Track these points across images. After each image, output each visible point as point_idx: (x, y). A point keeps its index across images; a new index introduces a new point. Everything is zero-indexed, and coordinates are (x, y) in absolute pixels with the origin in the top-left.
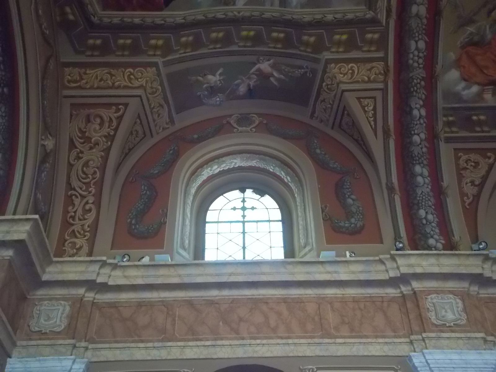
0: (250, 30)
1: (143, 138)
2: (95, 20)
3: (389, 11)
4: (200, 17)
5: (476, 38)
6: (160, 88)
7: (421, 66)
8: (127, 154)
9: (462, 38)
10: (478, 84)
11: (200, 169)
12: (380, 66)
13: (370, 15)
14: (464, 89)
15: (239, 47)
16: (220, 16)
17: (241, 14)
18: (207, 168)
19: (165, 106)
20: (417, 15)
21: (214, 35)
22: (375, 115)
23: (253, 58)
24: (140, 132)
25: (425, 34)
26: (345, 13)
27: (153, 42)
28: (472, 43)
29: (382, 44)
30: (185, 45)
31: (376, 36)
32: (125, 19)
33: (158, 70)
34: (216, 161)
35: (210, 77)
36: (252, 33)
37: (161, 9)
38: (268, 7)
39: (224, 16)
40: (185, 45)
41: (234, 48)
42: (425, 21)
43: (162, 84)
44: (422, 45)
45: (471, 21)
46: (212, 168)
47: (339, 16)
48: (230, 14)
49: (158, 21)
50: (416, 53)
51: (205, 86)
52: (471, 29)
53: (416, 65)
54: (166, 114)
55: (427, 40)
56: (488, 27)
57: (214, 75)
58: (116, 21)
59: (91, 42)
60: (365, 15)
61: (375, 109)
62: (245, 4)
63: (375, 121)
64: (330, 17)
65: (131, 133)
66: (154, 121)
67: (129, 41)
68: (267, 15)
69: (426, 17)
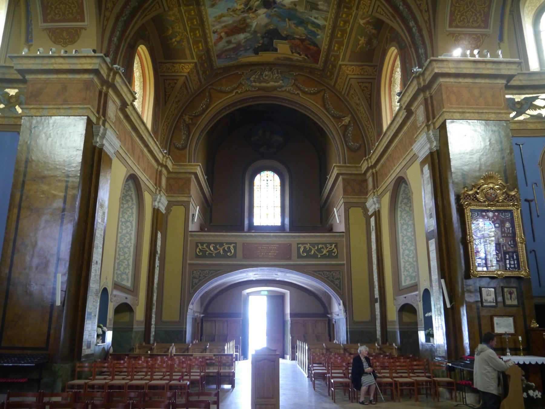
1: (371, 84)
4: (328, 39)
6: (352, 67)
8: (370, 98)
11: (392, 79)
15: (348, 27)
16: (330, 31)
18: (395, 74)
19: (364, 67)
21: (339, 36)
22: (385, 13)
24: (367, 85)
30: (339, 48)
33: (343, 65)
34: (394, 68)
35: (360, 42)
40: (339, 48)
41: (348, 30)
43: (351, 65)
46: (397, 71)
48: (330, 28)
51: (364, 45)
57: (360, 40)
61: (383, 11)
63: (388, 16)
65: (363, 90)
66: (368, 75)
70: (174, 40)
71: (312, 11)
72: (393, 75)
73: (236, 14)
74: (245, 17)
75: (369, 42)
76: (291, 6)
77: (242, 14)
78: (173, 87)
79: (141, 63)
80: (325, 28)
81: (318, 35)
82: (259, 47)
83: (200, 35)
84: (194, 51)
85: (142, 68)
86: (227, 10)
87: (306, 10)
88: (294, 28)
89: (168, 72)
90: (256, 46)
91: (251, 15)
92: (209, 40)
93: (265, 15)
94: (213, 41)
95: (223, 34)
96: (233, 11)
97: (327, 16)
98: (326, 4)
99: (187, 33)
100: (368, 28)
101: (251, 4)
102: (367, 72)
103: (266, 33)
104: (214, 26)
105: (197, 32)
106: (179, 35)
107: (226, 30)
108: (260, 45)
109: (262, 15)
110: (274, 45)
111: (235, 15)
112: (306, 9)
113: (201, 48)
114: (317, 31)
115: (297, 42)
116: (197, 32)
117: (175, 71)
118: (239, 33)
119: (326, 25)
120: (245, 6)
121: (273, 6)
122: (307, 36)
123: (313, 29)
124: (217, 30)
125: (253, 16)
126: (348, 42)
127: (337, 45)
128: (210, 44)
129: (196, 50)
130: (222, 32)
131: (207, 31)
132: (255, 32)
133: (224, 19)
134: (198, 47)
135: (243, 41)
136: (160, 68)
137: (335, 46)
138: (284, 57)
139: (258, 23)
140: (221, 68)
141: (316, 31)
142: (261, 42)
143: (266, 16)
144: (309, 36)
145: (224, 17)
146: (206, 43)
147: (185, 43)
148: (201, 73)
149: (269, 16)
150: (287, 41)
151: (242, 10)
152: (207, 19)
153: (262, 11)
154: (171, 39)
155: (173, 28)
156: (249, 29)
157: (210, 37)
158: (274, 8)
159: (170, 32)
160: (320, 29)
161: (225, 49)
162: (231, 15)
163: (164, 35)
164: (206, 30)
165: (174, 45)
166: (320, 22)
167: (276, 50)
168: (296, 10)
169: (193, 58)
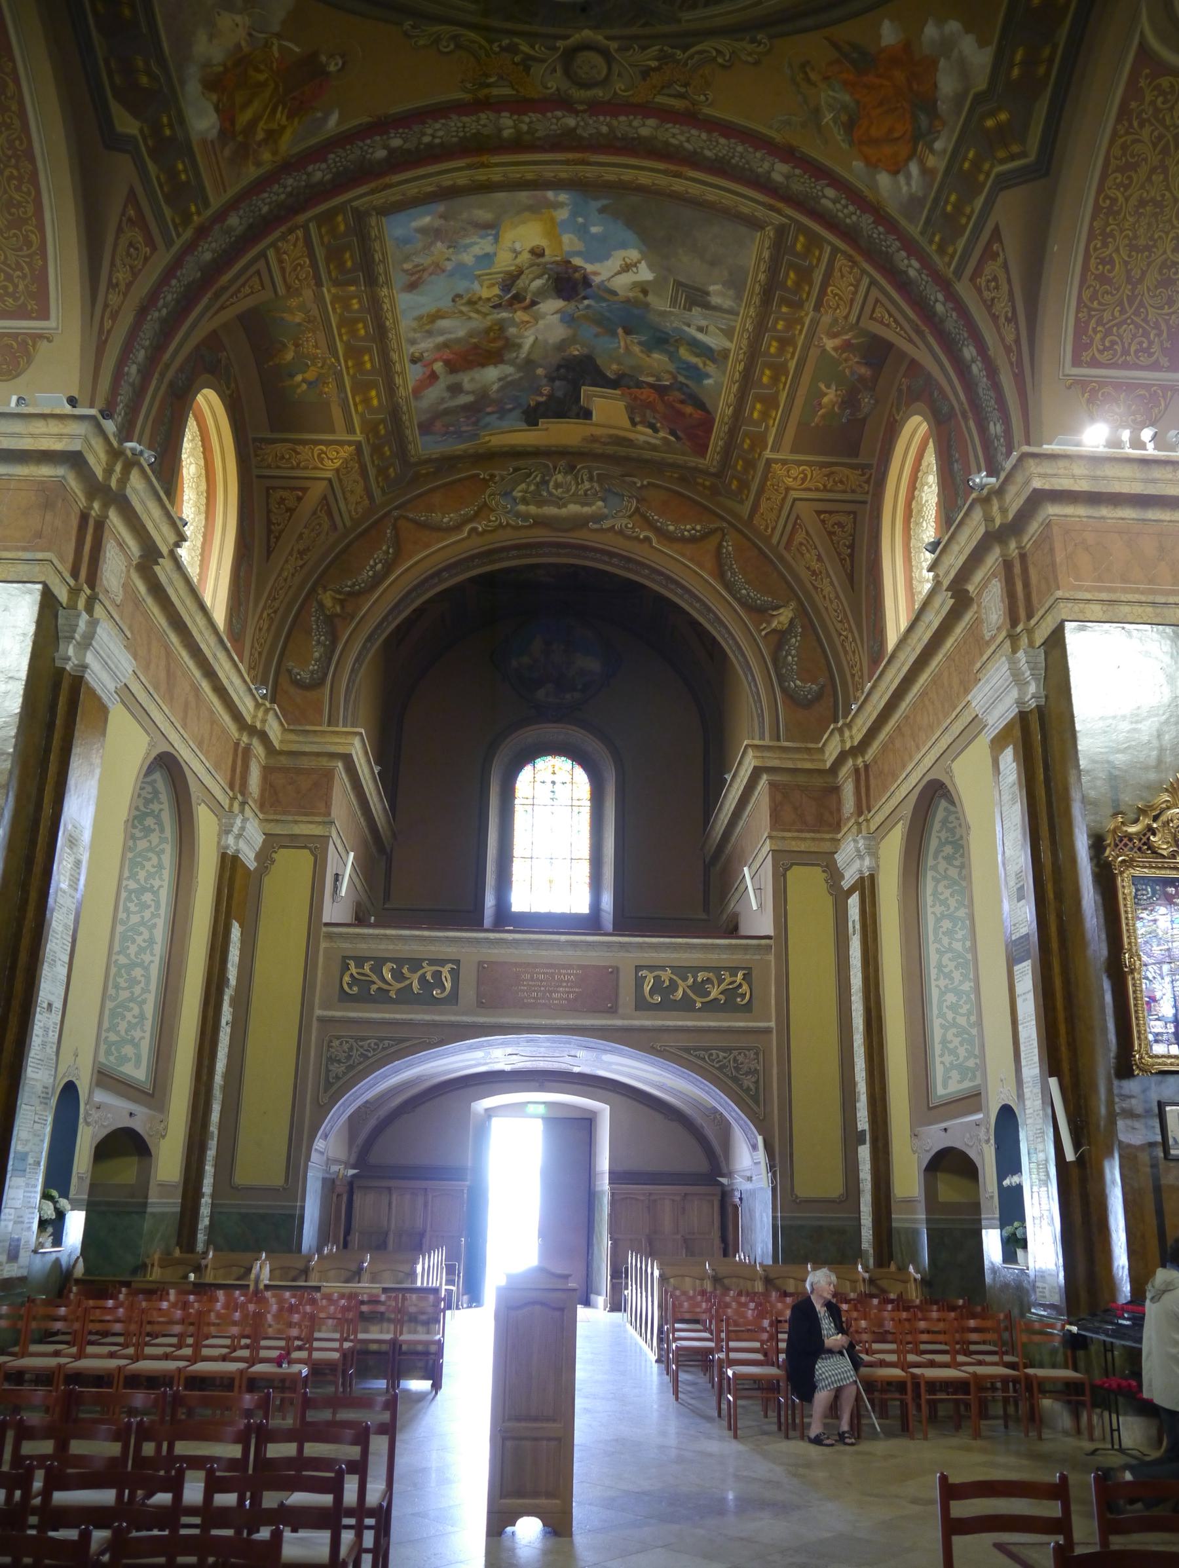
1: (855, 518)
3: (771, 208)
4: (735, 388)
5: (844, 118)
7: (858, 212)
8: (851, 556)
9: (839, 136)
10: (909, 158)
11: (914, 504)
12: (840, 261)
13: (770, 231)
14: (908, 184)
15: (792, 358)
16: (741, 367)
19: (834, 469)
20: (787, 177)
21: (765, 380)
22: (896, 321)
23: (814, 353)
24: (842, 518)
26: (760, 259)
28: (850, 126)
29: (814, 241)
30: (765, 415)
33: (776, 461)
34: (920, 474)
35: (825, 400)
37: (713, 420)
40: (765, 415)
41: (792, 365)
42: (798, 171)
43: (799, 463)
44: (830, 192)
45: (817, 112)
47: (763, 267)
48: (741, 357)
50: (839, 206)
52: (828, 117)
53: (854, 218)
54: (846, 471)
56: (831, 93)
57: (825, 394)
61: (890, 315)
63: (902, 329)
64: (762, 277)
65: (831, 534)
66: (845, 492)
69: (794, 168)
70: (299, 378)
71: (690, 310)
72: (916, 493)
73: (478, 312)
74: (503, 320)
75: (850, 401)
76: (631, 294)
78: (290, 511)
79: (203, 440)
80: (726, 357)
81: (708, 376)
82: (539, 404)
83: (373, 366)
84: (356, 410)
85: (204, 453)
86: (453, 301)
88: (640, 355)
89: (278, 467)
90: (532, 403)
91: (520, 316)
92: (398, 380)
93: (558, 316)
95: (438, 367)
96: (471, 303)
97: (733, 324)
98: (731, 292)
99: (338, 360)
100: (846, 360)
102: (841, 482)
103: (559, 367)
104: (413, 342)
105: (366, 358)
106: (314, 364)
107: (447, 354)
108: (543, 399)
110: (583, 401)
112: (674, 303)
113: (375, 402)
114: (705, 364)
115: (646, 394)
116: (366, 358)
117: (298, 464)
118: (483, 365)
119: (729, 350)
120: (502, 290)
122: (675, 378)
123: (694, 360)
124: (422, 354)
125: (526, 318)
126: (791, 398)
127: (758, 406)
128: (402, 392)
129: (360, 408)
130: (436, 360)
131: (395, 356)
132: (529, 364)
133: (443, 323)
134: (367, 401)
135: (495, 387)
136: (256, 455)
137: (753, 408)
138: (611, 436)
139: (540, 337)
140: (429, 461)
141: (701, 365)
142: (546, 390)
143: (562, 320)
144: (681, 379)
145: (443, 317)
146: (391, 388)
147: (330, 389)
148: (372, 472)
149: (569, 320)
150: (618, 392)
151: (497, 301)
152: (396, 322)
153: (551, 306)
154: (292, 376)
155: (297, 345)
156: (514, 355)
157: (403, 373)
158: (585, 298)
159: (289, 355)
160: (714, 361)
162: (461, 312)
163: (271, 364)
164: (392, 353)
165: (299, 391)
166: (714, 341)
167: (587, 414)
168: (647, 306)
169: (351, 430)
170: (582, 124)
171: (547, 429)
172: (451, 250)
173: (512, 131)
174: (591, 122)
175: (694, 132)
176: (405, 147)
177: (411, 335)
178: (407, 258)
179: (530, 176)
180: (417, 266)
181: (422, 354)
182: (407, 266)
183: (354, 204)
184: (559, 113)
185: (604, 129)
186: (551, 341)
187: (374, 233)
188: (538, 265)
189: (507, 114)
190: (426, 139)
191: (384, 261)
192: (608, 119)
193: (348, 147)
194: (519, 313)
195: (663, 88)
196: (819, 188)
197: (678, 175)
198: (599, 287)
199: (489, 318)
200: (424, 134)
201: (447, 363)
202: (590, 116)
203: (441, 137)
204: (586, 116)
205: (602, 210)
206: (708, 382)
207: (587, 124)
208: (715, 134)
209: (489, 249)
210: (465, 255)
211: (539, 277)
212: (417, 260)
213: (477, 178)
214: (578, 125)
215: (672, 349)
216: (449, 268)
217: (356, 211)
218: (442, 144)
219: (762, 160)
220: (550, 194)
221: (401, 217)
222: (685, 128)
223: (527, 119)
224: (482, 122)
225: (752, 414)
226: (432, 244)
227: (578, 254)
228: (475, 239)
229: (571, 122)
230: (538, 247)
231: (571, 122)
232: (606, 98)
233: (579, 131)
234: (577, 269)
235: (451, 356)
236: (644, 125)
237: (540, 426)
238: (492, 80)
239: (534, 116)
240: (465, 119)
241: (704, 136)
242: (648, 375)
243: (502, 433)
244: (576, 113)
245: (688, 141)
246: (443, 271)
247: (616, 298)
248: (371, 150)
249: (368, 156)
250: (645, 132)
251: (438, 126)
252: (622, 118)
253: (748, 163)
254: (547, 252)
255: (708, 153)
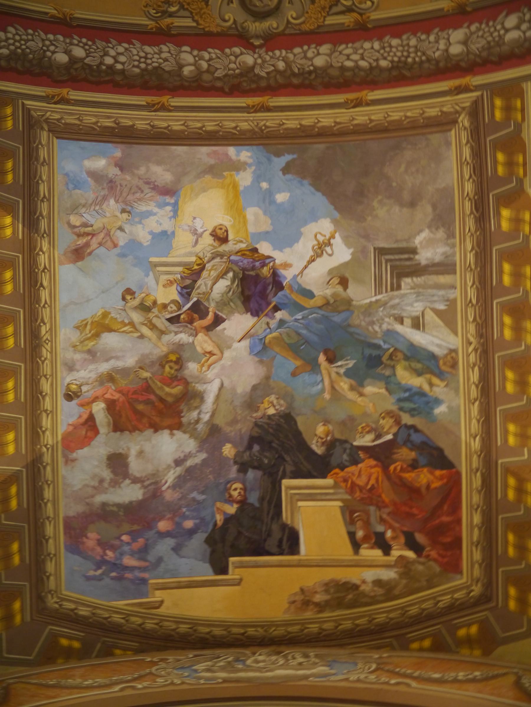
0: (502, 324)
2: (477, 590)
13: (464, 120)
16: (475, 376)
17: (472, 339)
21: (510, 388)
25: (494, 20)
26: (461, 163)
27: (511, 495)
31: (498, 102)
32: (475, 539)
36: (507, 320)
38: (456, 294)
39: (476, 369)
48: (472, 358)
49: (477, 482)
55: (504, 14)
58: (477, 556)
59: (512, 605)
60: (465, 128)
62: (456, 333)
64: (469, 187)
67: (511, 537)
68: (472, 294)
69: (468, 27)
71: (399, 287)
73: (153, 327)
74: (180, 347)
76: (329, 292)
77: (173, 328)
80: (454, 365)
81: (438, 402)
82: (228, 519)
86: (124, 299)
87: (380, 293)
88: (352, 395)
90: (219, 519)
92: (46, 422)
93: (246, 343)
94: (61, 430)
97: (452, 296)
98: (441, 234)
101: (203, 289)
103: (253, 440)
104: (71, 368)
107: (112, 393)
108: (232, 509)
109: (236, 345)
111: (145, 330)
112: (379, 287)
114: (431, 385)
118: (156, 428)
120: (180, 294)
121: (274, 301)
122: (398, 421)
124: (80, 386)
125: (209, 347)
127: (512, 428)
128: (48, 439)
130: (95, 399)
131: (46, 386)
135: (171, 477)
138: (327, 586)
139: (226, 384)
141: (426, 387)
143: (251, 348)
144: (407, 419)
145: (110, 330)
150: (329, 481)
152: (53, 331)
157: (53, 413)
158: (276, 309)
160: (440, 375)
161: (100, 499)
162: (132, 324)
168: (349, 302)
170: (259, 61)
171: (239, 582)
172: (125, 216)
173: (192, 68)
174: (268, 58)
175: (367, 45)
176: (86, 61)
177: (70, 355)
178: (74, 209)
179: (210, 127)
180: (85, 225)
181: (80, 386)
182: (75, 220)
183: (28, 103)
184: (237, 50)
185: (281, 65)
186: (239, 390)
187: (43, 153)
188: (221, 255)
189: (186, 48)
190: (109, 61)
191: (49, 199)
192: (284, 52)
193: (30, 31)
194: (201, 336)
195: (331, 7)
196: (499, 27)
197: (358, 103)
198: (291, 287)
199: (166, 338)
200: (106, 54)
201: (111, 406)
202: (267, 52)
203: (123, 64)
204: (262, 51)
205: (286, 170)
206: (440, 410)
207: (264, 61)
208: (387, 38)
209: (167, 225)
210: (140, 226)
211: (222, 275)
212: (88, 217)
213: (156, 123)
214: (255, 63)
215: (387, 372)
216: (121, 243)
217: (27, 111)
218: (123, 71)
219: (437, 41)
220: (231, 151)
221: (74, 147)
222: (357, 45)
223: (206, 56)
224: (164, 55)
225: (506, 441)
226: (105, 198)
227: (265, 236)
228: (151, 207)
229: (249, 59)
230: (220, 227)
231: (249, 59)
232: (281, 28)
233: (257, 71)
234: (265, 260)
235: (117, 396)
236: (318, 54)
237: (233, 574)
238: (173, 9)
239: (214, 52)
240: (147, 49)
241: (377, 45)
242: (363, 434)
243: (179, 586)
244: (253, 48)
245: (363, 58)
246: (115, 246)
247: (312, 303)
248: (52, 48)
249: (49, 54)
250: (319, 62)
251: (121, 49)
252: (297, 50)
253: (424, 54)
254: (230, 237)
255: (384, 63)
